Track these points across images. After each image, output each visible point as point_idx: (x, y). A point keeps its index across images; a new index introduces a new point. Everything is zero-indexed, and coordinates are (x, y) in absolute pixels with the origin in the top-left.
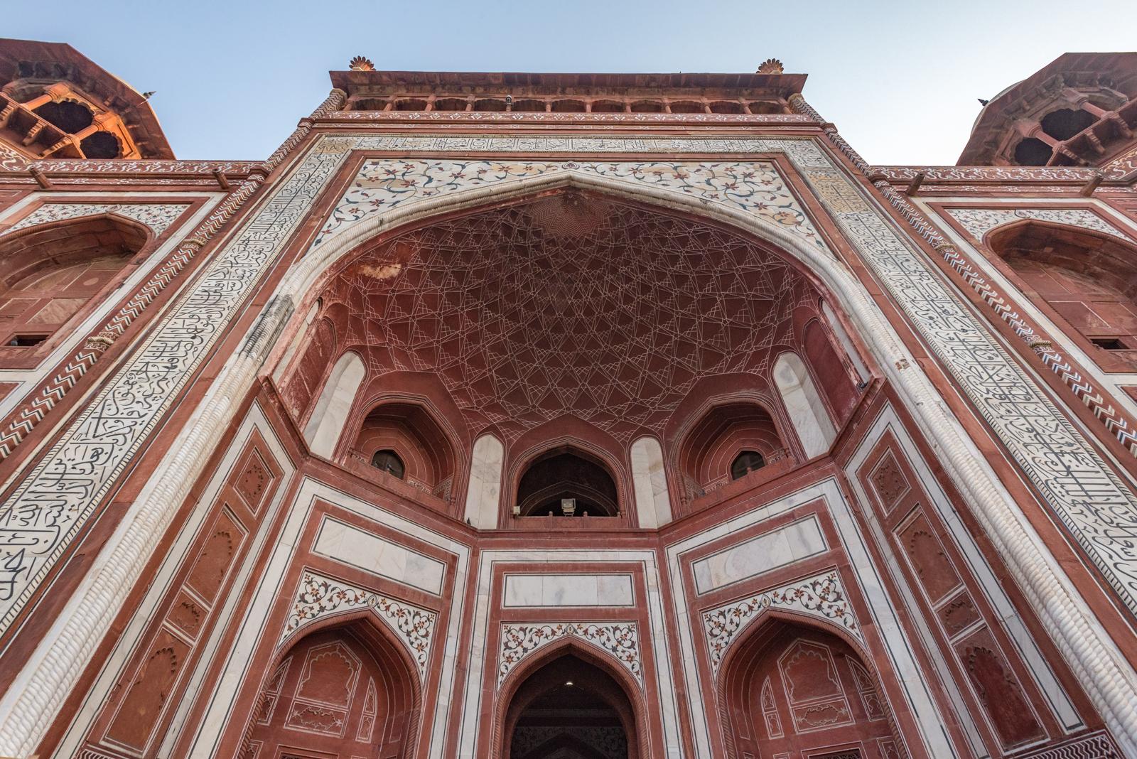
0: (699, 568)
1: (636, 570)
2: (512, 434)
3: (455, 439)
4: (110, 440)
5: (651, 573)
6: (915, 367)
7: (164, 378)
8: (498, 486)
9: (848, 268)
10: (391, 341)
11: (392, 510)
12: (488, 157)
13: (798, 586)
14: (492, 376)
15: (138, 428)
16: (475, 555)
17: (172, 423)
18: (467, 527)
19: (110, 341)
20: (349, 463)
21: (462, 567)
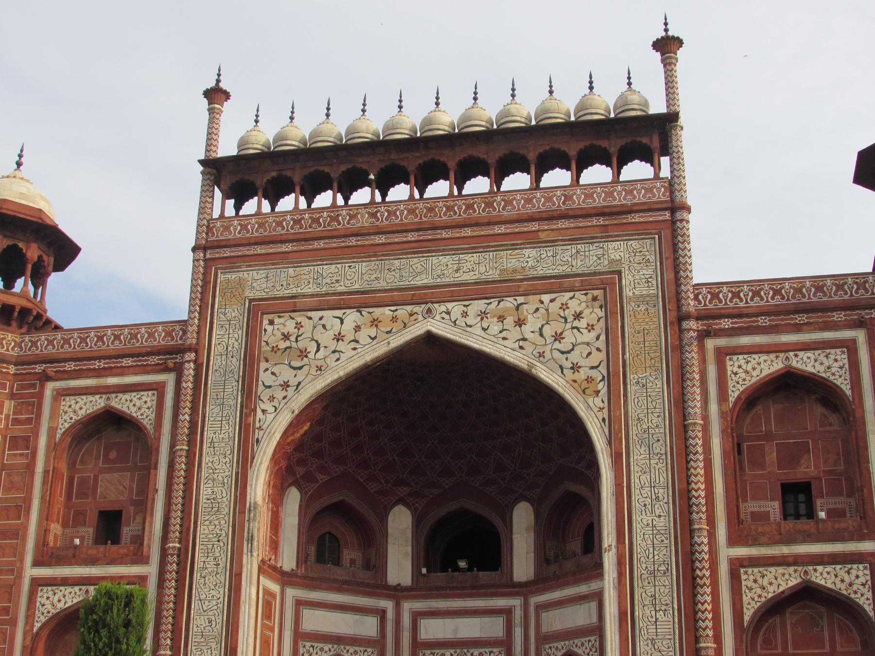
0: (544, 615)
1: (507, 612)
2: (417, 502)
3: (373, 519)
4: (211, 613)
5: (518, 614)
6: (614, 550)
7: (217, 573)
8: (410, 549)
9: (611, 455)
10: (312, 464)
11: (339, 590)
12: (361, 300)
13: (583, 640)
14: (394, 459)
15: (220, 606)
16: (398, 606)
17: (234, 604)
18: (387, 587)
19: (178, 545)
20: (306, 569)
21: (390, 615)
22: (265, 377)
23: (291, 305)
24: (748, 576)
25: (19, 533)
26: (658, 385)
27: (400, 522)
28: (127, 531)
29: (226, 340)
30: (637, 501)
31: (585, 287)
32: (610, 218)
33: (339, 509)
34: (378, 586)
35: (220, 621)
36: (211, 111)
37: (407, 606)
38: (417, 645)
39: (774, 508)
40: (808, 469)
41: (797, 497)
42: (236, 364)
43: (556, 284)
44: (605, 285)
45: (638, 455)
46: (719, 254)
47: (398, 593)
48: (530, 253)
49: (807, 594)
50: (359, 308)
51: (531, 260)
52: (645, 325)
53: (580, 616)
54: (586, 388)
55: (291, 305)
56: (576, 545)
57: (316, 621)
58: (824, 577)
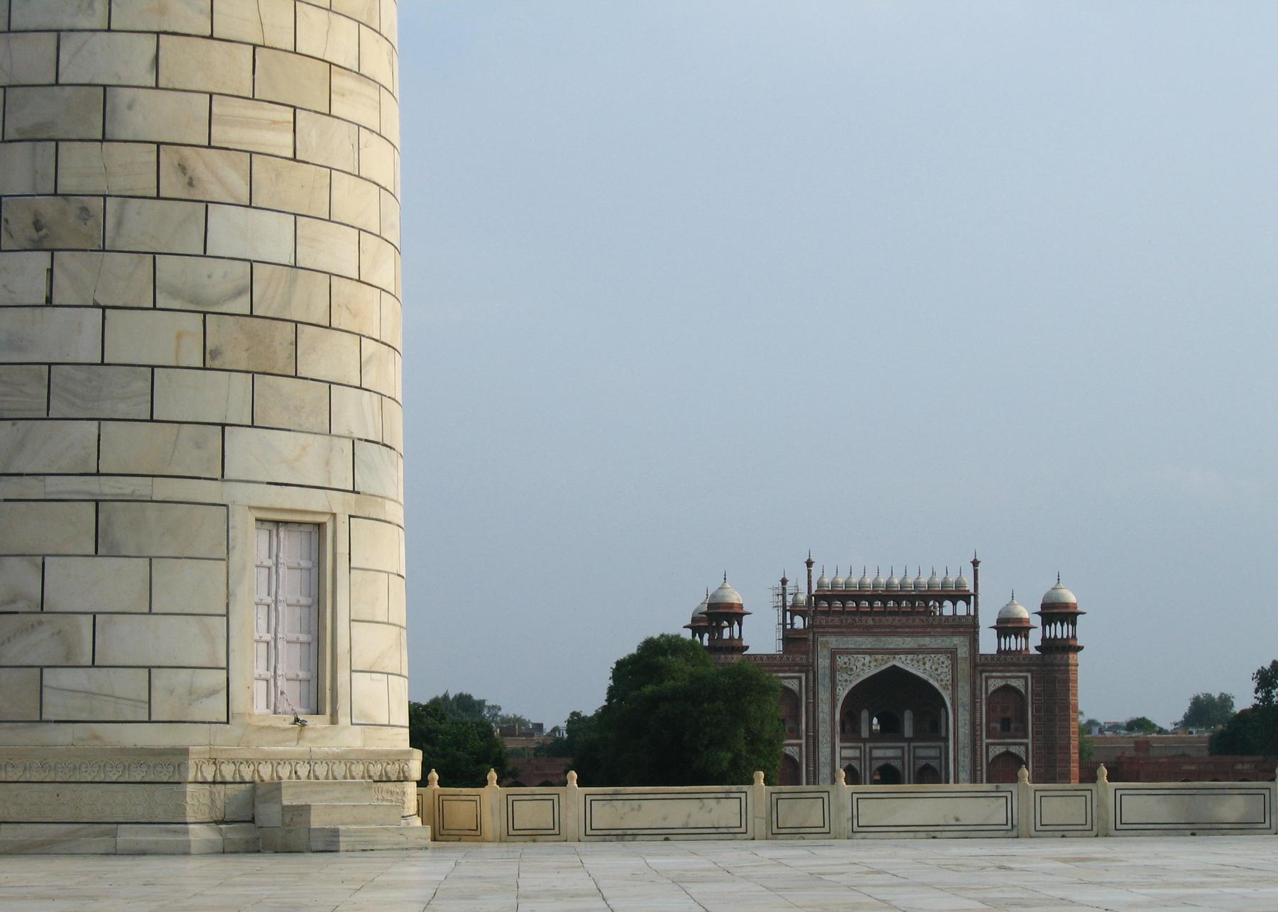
1: (903, 748)
12: (870, 652)
22: (839, 677)
23: (847, 652)
24: (991, 748)
26: (968, 688)
29: (823, 663)
31: (945, 653)
34: (860, 739)
35: (829, 759)
36: (809, 571)
37: (868, 745)
38: (871, 758)
39: (998, 726)
40: (1009, 714)
41: (1006, 724)
42: (828, 672)
43: (937, 651)
44: (952, 653)
45: (961, 710)
47: (865, 741)
48: (928, 639)
49: (1008, 753)
50: (870, 654)
51: (927, 641)
52: (964, 667)
53: (933, 753)
55: (847, 652)
58: (1013, 749)
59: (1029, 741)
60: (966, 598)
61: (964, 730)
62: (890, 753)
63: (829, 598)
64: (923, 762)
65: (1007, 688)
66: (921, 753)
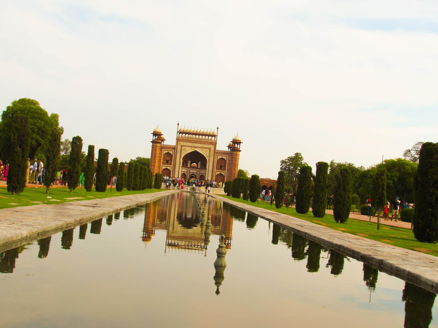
23: (185, 146)
25: (161, 162)
26: (213, 157)
27: (189, 162)
28: (169, 162)
29: (179, 148)
30: (210, 165)
32: (211, 143)
33: (185, 161)
40: (222, 165)
41: (221, 167)
42: (180, 150)
43: (206, 148)
44: (210, 149)
46: (218, 148)
47: (189, 168)
52: (212, 152)
53: (204, 172)
54: (207, 157)
55: (185, 146)
56: (204, 166)
57: (183, 170)
58: (222, 173)
59: (226, 171)
60: (215, 136)
61: (211, 167)
62: (194, 171)
63: (182, 133)
64: (201, 174)
65: (222, 158)
66: (201, 172)
